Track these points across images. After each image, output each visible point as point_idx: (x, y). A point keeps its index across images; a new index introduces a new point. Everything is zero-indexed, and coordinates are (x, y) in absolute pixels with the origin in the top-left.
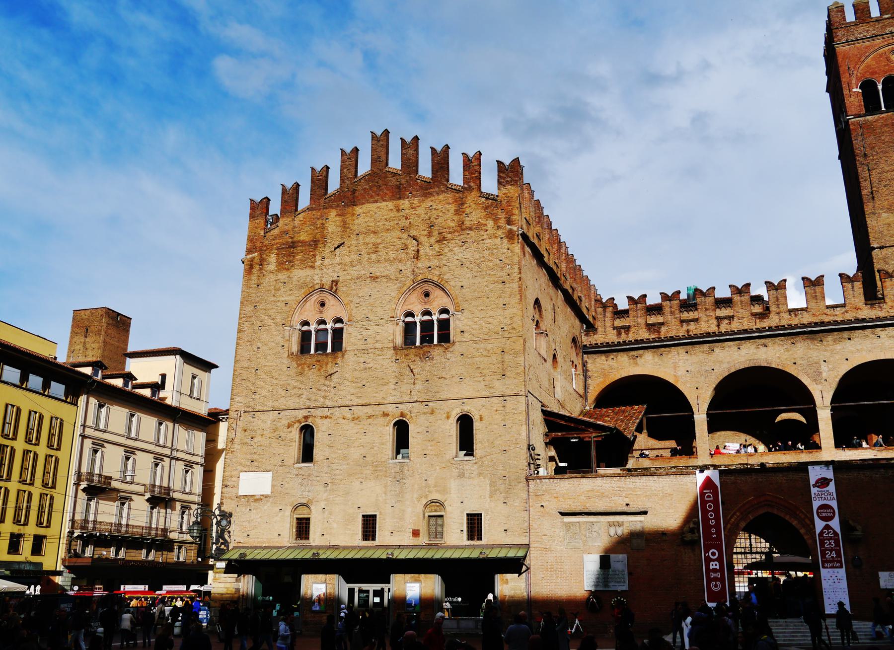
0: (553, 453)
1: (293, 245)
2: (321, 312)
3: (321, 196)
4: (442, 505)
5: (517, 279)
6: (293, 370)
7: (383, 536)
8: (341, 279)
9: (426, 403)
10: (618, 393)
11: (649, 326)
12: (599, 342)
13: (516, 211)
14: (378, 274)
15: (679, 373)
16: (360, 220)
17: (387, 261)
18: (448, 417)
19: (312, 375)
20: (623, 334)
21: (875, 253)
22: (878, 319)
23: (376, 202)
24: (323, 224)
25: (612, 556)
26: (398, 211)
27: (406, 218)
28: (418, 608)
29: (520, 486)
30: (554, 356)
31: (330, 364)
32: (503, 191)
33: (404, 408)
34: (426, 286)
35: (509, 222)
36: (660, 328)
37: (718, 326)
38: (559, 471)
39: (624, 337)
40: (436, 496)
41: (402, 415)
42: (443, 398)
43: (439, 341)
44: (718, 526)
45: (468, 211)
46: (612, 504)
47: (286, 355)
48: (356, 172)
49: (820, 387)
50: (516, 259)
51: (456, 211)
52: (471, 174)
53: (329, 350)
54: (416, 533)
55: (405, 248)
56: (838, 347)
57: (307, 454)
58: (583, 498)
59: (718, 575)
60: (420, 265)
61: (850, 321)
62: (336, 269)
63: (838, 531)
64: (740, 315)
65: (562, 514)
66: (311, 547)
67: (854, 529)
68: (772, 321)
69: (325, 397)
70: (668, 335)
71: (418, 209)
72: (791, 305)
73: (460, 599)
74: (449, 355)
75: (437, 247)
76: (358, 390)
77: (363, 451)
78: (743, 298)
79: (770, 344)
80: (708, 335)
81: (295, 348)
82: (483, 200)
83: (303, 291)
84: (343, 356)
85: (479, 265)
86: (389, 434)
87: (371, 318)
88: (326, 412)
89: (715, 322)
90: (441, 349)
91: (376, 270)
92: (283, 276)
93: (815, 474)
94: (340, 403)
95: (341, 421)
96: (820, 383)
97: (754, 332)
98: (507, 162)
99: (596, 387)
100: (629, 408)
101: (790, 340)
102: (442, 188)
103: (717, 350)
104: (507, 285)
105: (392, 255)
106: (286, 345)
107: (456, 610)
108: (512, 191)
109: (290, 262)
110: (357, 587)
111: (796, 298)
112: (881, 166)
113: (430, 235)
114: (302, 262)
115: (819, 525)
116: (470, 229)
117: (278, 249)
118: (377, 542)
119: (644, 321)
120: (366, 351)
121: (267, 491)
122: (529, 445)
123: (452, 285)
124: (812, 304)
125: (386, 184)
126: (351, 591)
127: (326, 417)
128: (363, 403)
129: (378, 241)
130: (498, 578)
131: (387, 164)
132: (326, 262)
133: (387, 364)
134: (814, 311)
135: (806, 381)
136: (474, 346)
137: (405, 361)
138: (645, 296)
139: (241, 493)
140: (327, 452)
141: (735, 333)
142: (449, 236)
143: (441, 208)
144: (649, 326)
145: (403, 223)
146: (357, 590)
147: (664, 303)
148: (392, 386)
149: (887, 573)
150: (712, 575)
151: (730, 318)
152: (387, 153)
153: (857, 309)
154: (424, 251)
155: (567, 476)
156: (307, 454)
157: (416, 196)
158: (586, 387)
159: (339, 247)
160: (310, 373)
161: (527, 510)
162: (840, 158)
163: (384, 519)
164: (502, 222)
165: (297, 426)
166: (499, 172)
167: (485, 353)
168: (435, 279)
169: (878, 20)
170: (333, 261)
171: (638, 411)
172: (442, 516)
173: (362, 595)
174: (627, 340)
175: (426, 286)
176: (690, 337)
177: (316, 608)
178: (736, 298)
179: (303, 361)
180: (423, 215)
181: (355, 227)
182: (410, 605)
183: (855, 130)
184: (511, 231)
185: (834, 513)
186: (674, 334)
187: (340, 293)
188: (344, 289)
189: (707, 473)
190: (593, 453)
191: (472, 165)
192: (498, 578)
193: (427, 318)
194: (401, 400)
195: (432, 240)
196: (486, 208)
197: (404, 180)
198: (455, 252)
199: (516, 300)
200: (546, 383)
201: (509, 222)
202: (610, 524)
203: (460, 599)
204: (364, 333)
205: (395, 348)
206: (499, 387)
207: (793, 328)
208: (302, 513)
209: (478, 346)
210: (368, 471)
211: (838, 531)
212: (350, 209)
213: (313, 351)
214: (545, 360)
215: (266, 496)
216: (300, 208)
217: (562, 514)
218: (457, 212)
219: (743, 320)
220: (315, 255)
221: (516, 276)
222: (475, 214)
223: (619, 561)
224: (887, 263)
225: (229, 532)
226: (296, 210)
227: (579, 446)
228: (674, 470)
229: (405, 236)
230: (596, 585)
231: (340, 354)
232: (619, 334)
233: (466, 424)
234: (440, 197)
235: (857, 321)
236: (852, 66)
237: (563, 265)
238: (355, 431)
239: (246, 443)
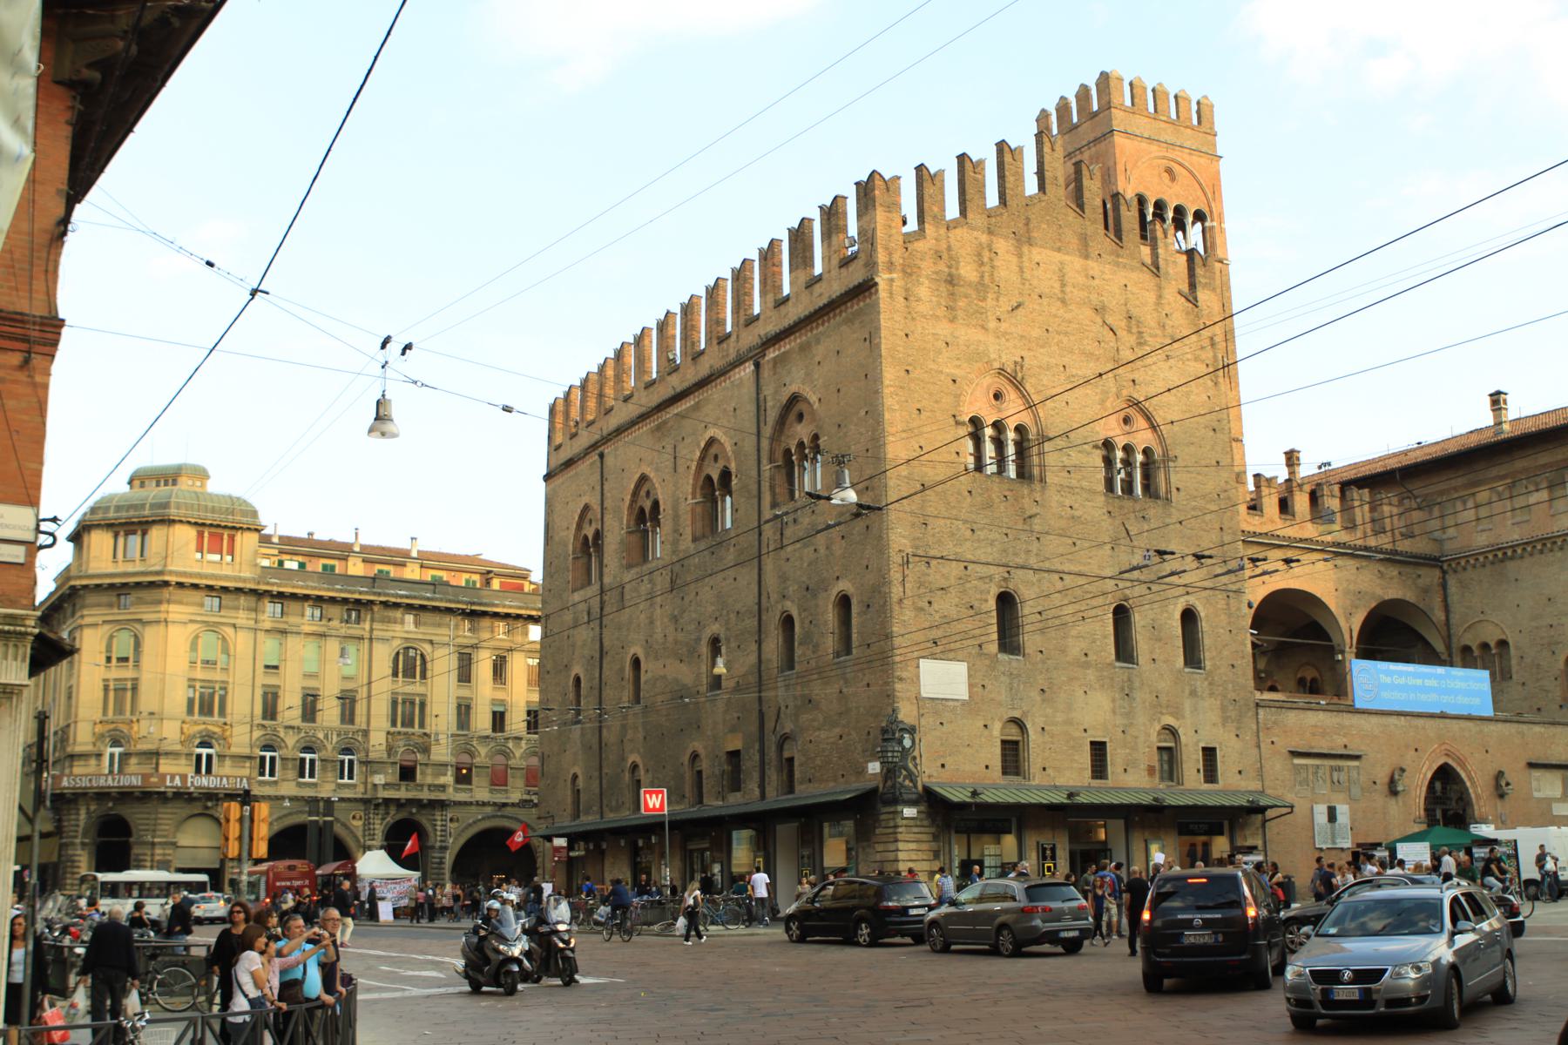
40: (1170, 720)
54: (1151, 770)
77: (1083, 645)
94: (1047, 565)
118: (1109, 782)
121: (962, 692)
129: (1068, 316)
132: (1004, 326)
139: (924, 694)
153: (1273, 522)
202: (1333, 769)
208: (1013, 734)
210: (1091, 675)
215: (964, 703)
217: (1295, 754)
225: (914, 758)
239: (922, 609)
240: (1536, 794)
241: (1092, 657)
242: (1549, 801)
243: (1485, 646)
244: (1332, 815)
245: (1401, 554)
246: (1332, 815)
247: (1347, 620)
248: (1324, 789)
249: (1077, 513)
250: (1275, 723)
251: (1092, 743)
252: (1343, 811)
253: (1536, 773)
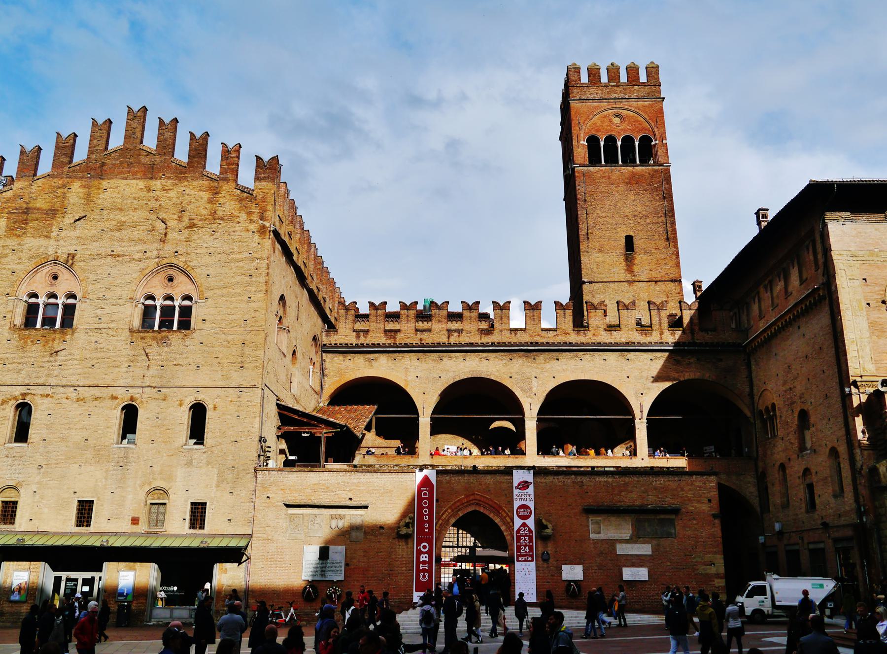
0: (284, 446)
1: (27, 211)
2: (52, 285)
3: (65, 164)
4: (166, 492)
5: (264, 274)
6: (15, 344)
7: (98, 522)
8: (79, 253)
9: (159, 388)
10: (351, 393)
11: (386, 332)
12: (338, 343)
13: (270, 208)
14: (120, 253)
15: (410, 378)
16: (106, 195)
17: (131, 240)
18: (181, 405)
19: (35, 351)
20: (362, 337)
21: (584, 286)
22: (583, 344)
23: (126, 178)
24: (64, 193)
25: (331, 547)
26: (149, 191)
27: (157, 200)
28: (130, 598)
29: (248, 476)
30: (294, 352)
31: (57, 341)
32: (259, 186)
33: (134, 392)
34: (171, 271)
35: (262, 218)
36: (396, 335)
37: (449, 337)
38: (288, 464)
39: (362, 340)
41: (132, 399)
42: (176, 385)
43: (179, 327)
44: (430, 522)
45: (222, 201)
47: (7, 327)
48: (107, 144)
49: (530, 400)
50: (265, 255)
51: (209, 199)
52: (228, 165)
53: (58, 326)
54: (135, 521)
55: (152, 229)
56: (548, 366)
57: (22, 433)
58: (309, 491)
59: (427, 567)
60: (166, 248)
61: (559, 344)
62: (74, 242)
63: (533, 529)
64: (468, 329)
65: (287, 506)
66: (16, 533)
67: (546, 527)
68: (495, 337)
69: (48, 375)
70: (403, 342)
71: (170, 192)
72: (513, 324)
73: (175, 588)
74: (188, 342)
75: (186, 233)
76: (86, 370)
77: (85, 434)
78: (472, 314)
79: (491, 358)
80: (439, 345)
81: (19, 320)
82: (239, 192)
83: (34, 261)
84: (73, 333)
85: (228, 256)
86: (116, 418)
87: (108, 297)
88: (47, 390)
89: (446, 333)
90: (180, 336)
91: (118, 248)
92: (12, 242)
93: (518, 477)
94: (64, 382)
95: (64, 401)
96: (530, 396)
97: (479, 346)
98: (266, 158)
99: (332, 385)
100: (361, 407)
101: (508, 356)
102: (197, 175)
103: (445, 359)
104: (254, 279)
105: (137, 234)
106: (9, 316)
107: (170, 601)
108: (268, 187)
109: (22, 229)
110: (64, 575)
111: (517, 319)
112: (597, 211)
113: (180, 219)
114: (36, 230)
115: (518, 522)
116: (222, 219)
117: (9, 213)
118: (92, 529)
119: (382, 327)
120: (99, 330)
122: (261, 438)
123: (198, 273)
124: (530, 326)
125: (139, 162)
126: (58, 580)
127: (47, 396)
128: (91, 384)
129: (125, 219)
130: (217, 567)
131: (141, 142)
133: (120, 346)
134: (531, 332)
135: (518, 394)
136: (215, 335)
137: (140, 344)
138: (385, 303)
140: (45, 433)
141: (463, 346)
142: (200, 223)
143: (195, 194)
144: (386, 332)
145: (152, 204)
146: (64, 578)
147: (402, 312)
148: (124, 369)
149: (568, 567)
150: (422, 567)
151: (460, 331)
152: (143, 131)
153: (566, 333)
154: (173, 234)
155: (295, 469)
156: (22, 433)
157: (169, 178)
158: (322, 385)
159: (79, 219)
160: (34, 348)
161: (253, 501)
162: (564, 200)
163: (102, 505)
164: (255, 217)
165: (13, 404)
166: (257, 167)
167: (225, 343)
168: (181, 264)
169: (605, 86)
170: (72, 234)
171: (368, 412)
172: (165, 504)
173: (69, 584)
174: (365, 343)
175: (171, 271)
176: (423, 346)
177: (15, 597)
178: (466, 314)
179: (27, 335)
180: (174, 199)
181: (100, 201)
182: (121, 594)
183: (579, 177)
184: (263, 226)
185: (531, 513)
186: (408, 341)
187: (75, 268)
188: (81, 264)
189: (426, 472)
190: (323, 448)
191: (230, 156)
192: (217, 567)
193: (168, 303)
194: (132, 384)
195: (182, 225)
196: (241, 200)
197: (158, 160)
198: (204, 240)
199: (261, 294)
200: (283, 377)
201: (262, 218)
202: (333, 517)
203: (175, 588)
204: (99, 312)
205: (131, 331)
206: (237, 378)
207: (512, 345)
209: (218, 336)
211: (533, 529)
212: (96, 182)
213: (39, 325)
214: (285, 355)
216: (40, 173)
217: (287, 506)
218: (211, 201)
219: (471, 334)
220: (51, 225)
221: (263, 270)
222: (228, 204)
223: (338, 553)
224: (594, 296)
226: (35, 175)
227: (308, 441)
228: (396, 468)
229: (153, 217)
230: (314, 575)
231: (69, 331)
232: (358, 337)
233: (198, 412)
234: (195, 183)
235: (565, 344)
236: (582, 122)
237: (311, 265)
238: (79, 413)
240: (593, 536)
241: (91, 442)
242: (612, 543)
243: (767, 408)
245: (700, 344)
247: (637, 397)
249: (101, 346)
251: (79, 501)
253: (592, 518)
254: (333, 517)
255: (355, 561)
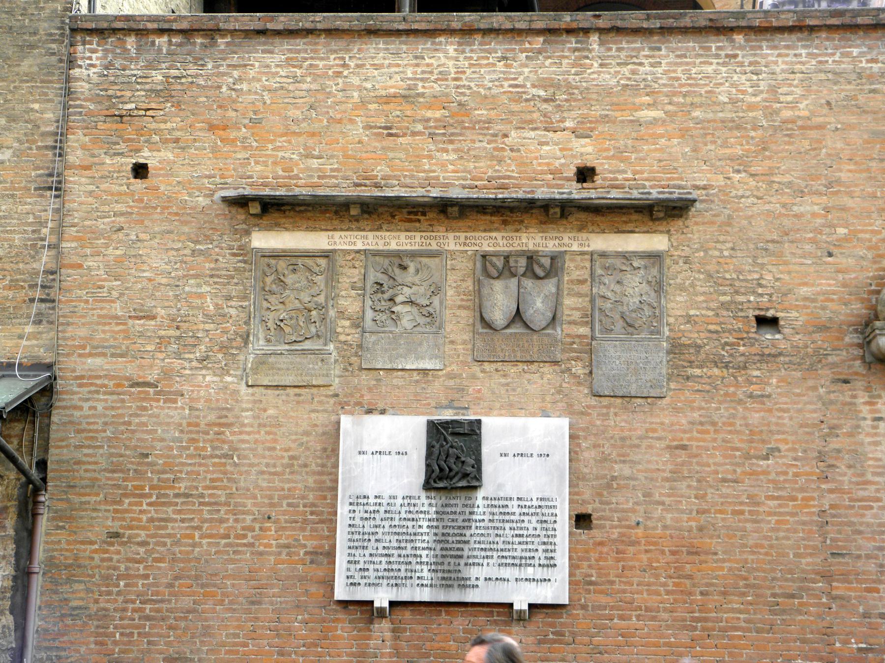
46: (510, 169)
58: (357, 131)
161: (55, 186)
202: (494, 268)
244: (453, 458)
246: (453, 458)
248: (441, 361)
250: (164, 93)
252: (528, 451)
254: (494, 268)
255: (623, 500)
